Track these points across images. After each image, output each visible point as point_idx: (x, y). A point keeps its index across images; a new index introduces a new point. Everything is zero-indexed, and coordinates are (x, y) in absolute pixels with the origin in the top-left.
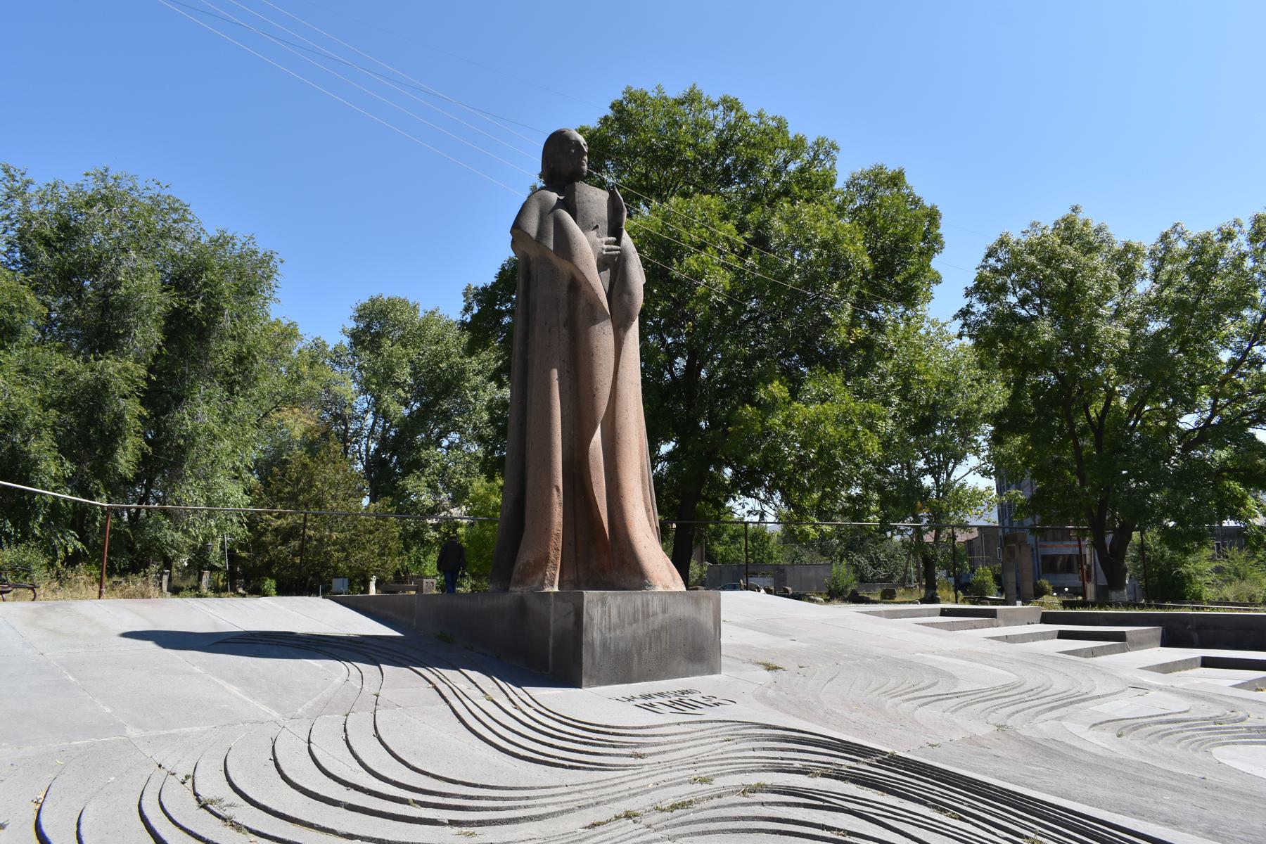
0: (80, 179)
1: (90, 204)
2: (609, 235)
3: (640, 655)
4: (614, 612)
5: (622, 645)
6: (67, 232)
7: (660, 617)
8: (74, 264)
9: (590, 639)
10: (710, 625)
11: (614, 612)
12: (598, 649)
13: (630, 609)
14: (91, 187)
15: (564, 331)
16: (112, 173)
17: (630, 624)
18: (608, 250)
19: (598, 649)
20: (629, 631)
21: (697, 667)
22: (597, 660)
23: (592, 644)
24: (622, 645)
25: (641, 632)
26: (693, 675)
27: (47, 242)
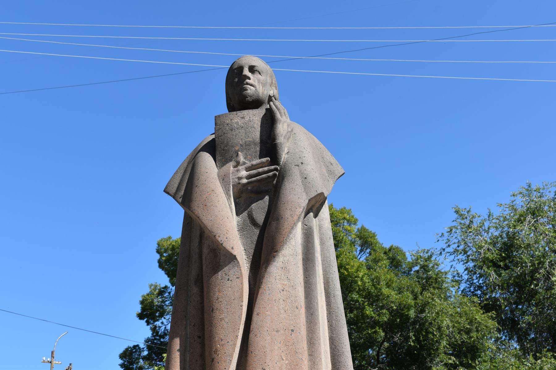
0: (507, 200)
1: (520, 221)
2: (260, 157)
6: (508, 248)
8: (518, 277)
14: (520, 203)
15: (195, 290)
16: (534, 187)
18: (248, 177)
27: (495, 264)
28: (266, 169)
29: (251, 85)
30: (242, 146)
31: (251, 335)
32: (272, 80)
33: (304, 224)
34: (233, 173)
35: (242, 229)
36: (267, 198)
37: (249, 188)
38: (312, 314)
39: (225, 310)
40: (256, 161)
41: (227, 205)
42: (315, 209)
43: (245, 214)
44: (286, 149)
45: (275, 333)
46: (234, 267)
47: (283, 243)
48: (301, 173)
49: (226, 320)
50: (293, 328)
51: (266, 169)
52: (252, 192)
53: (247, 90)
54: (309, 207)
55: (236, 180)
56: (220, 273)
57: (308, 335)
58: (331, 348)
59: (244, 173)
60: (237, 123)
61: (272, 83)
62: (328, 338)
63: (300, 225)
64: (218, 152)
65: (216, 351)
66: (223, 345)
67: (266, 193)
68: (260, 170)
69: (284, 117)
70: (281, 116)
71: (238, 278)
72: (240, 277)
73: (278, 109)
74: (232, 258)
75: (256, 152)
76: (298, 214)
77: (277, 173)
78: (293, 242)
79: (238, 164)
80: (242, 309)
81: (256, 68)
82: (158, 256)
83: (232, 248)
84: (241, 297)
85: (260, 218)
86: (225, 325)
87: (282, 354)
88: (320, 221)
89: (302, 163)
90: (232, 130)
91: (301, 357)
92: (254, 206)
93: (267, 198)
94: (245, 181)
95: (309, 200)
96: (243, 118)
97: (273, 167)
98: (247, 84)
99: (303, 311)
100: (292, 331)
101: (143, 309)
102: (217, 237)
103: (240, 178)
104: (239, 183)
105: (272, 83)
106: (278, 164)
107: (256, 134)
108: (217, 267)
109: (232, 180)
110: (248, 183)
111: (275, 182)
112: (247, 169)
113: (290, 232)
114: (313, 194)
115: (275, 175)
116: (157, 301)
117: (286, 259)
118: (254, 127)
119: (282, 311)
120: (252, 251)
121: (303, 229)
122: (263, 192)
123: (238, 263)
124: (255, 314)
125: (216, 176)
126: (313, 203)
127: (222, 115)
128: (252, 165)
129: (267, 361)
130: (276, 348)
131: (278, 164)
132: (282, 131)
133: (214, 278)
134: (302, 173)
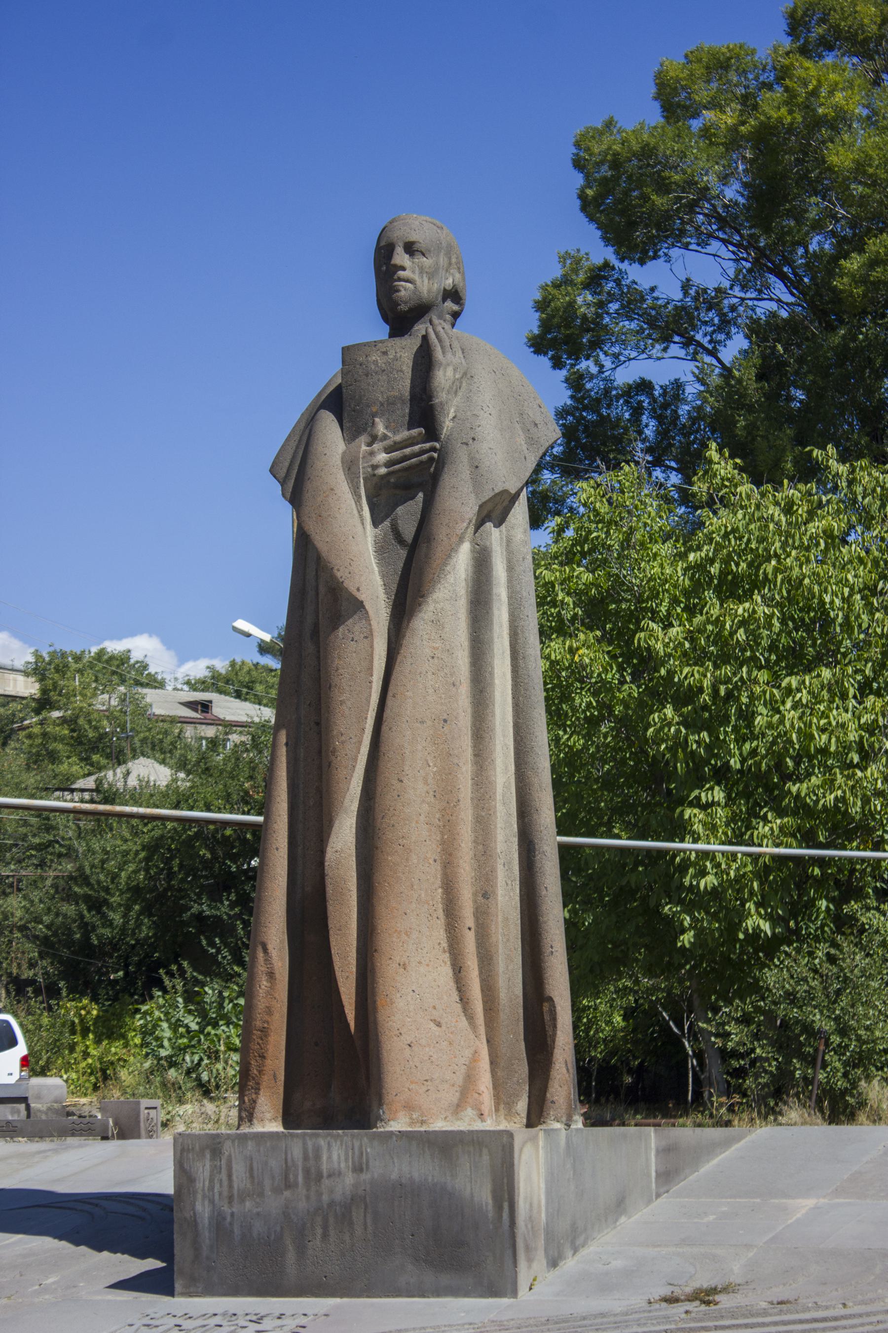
3: (301, 1251)
4: (239, 1170)
5: (258, 1227)
7: (349, 1179)
9: (188, 1214)
10: (483, 1194)
11: (239, 1170)
12: (206, 1235)
13: (275, 1164)
15: (310, 647)
17: (277, 1191)
18: (389, 464)
19: (206, 1235)
20: (273, 1204)
21: (445, 1279)
22: (205, 1251)
23: (194, 1223)
24: (258, 1227)
25: (302, 1205)
26: (438, 1292)
28: (417, 448)
29: (407, 281)
30: (382, 405)
31: (384, 728)
32: (450, 258)
33: (474, 543)
34: (364, 457)
35: (381, 550)
36: (421, 495)
37: (392, 480)
38: (481, 691)
39: (347, 688)
40: (404, 434)
41: (355, 512)
42: (495, 514)
43: (387, 523)
44: (452, 410)
45: (418, 725)
46: (360, 619)
47: (434, 582)
48: (471, 458)
49: (349, 704)
50: (445, 717)
51: (417, 448)
52: (396, 486)
53: (398, 291)
54: (485, 512)
55: (369, 470)
56: (341, 629)
57: (474, 725)
58: (515, 740)
59: (382, 457)
60: (375, 362)
61: (450, 264)
62: (511, 724)
63: (466, 548)
64: (345, 415)
65: (334, 752)
66: (343, 743)
67: (420, 486)
68: (408, 451)
69: (449, 355)
70: (444, 353)
71: (366, 637)
72: (369, 636)
73: (440, 341)
74: (359, 606)
75: (404, 416)
76: (459, 532)
77: (435, 455)
78: (451, 578)
79: (374, 439)
80: (371, 688)
81: (416, 247)
82: (579, 179)
83: (358, 590)
84: (370, 669)
85: (409, 531)
86: (347, 712)
87: (429, 758)
88: (508, 531)
89: (474, 439)
90: (367, 375)
91: (456, 761)
92: (400, 510)
93: (421, 495)
94: (383, 471)
95: (481, 506)
96: (385, 353)
97: (427, 445)
98: (400, 279)
99: (464, 690)
100: (445, 721)
101: (546, 326)
102: (335, 571)
103: (375, 467)
104: (374, 475)
105: (450, 264)
106: (437, 439)
107: (404, 385)
108: (337, 620)
109: (363, 468)
110: (389, 474)
111: (432, 469)
112: (388, 450)
113: (445, 564)
114: (487, 495)
115: (431, 459)
116: (584, 300)
117: (438, 606)
118: (401, 371)
119: (431, 691)
120: (394, 587)
121: (473, 551)
122: (409, 489)
123: (367, 613)
124: (390, 694)
125: (339, 462)
126: (489, 507)
127: (353, 346)
128: (395, 443)
129: (406, 768)
130: (420, 747)
131: (437, 439)
132: (443, 381)
133: (332, 636)
134: (472, 458)
